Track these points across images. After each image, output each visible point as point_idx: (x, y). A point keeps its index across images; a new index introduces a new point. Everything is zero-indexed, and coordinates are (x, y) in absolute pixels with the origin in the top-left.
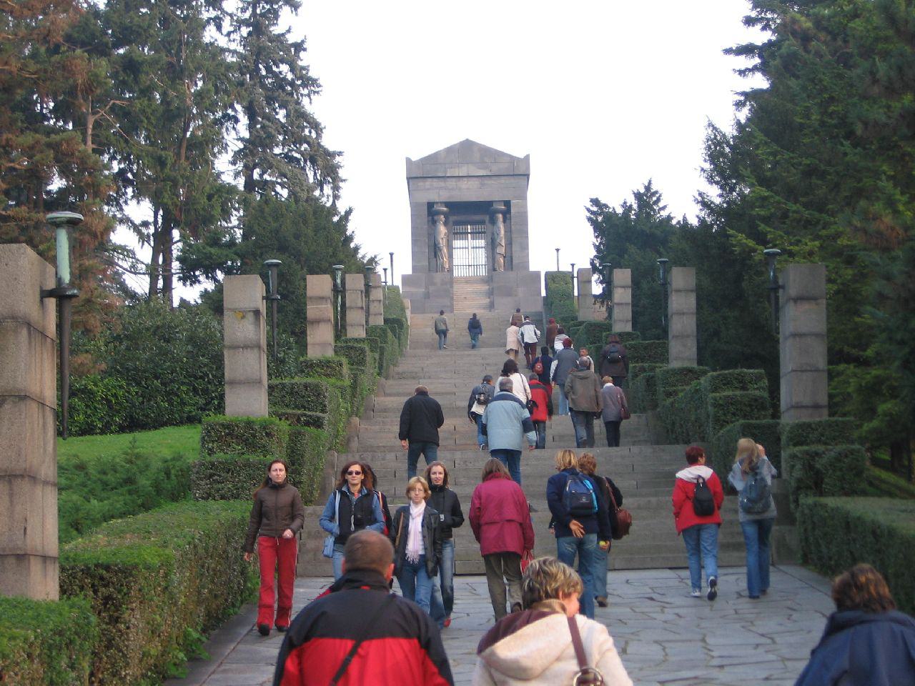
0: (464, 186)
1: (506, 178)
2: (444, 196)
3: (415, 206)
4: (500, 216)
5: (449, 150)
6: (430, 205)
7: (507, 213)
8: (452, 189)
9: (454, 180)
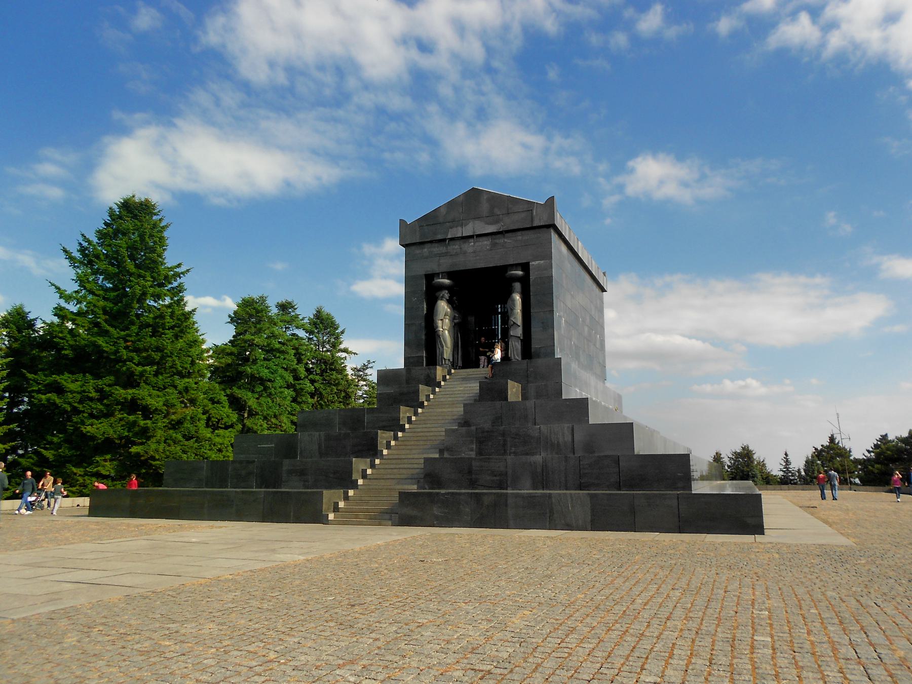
0: (470, 250)
1: (523, 232)
2: (446, 264)
3: (410, 281)
4: (517, 286)
5: (451, 204)
6: (430, 277)
7: (525, 281)
8: (457, 254)
9: (458, 242)
